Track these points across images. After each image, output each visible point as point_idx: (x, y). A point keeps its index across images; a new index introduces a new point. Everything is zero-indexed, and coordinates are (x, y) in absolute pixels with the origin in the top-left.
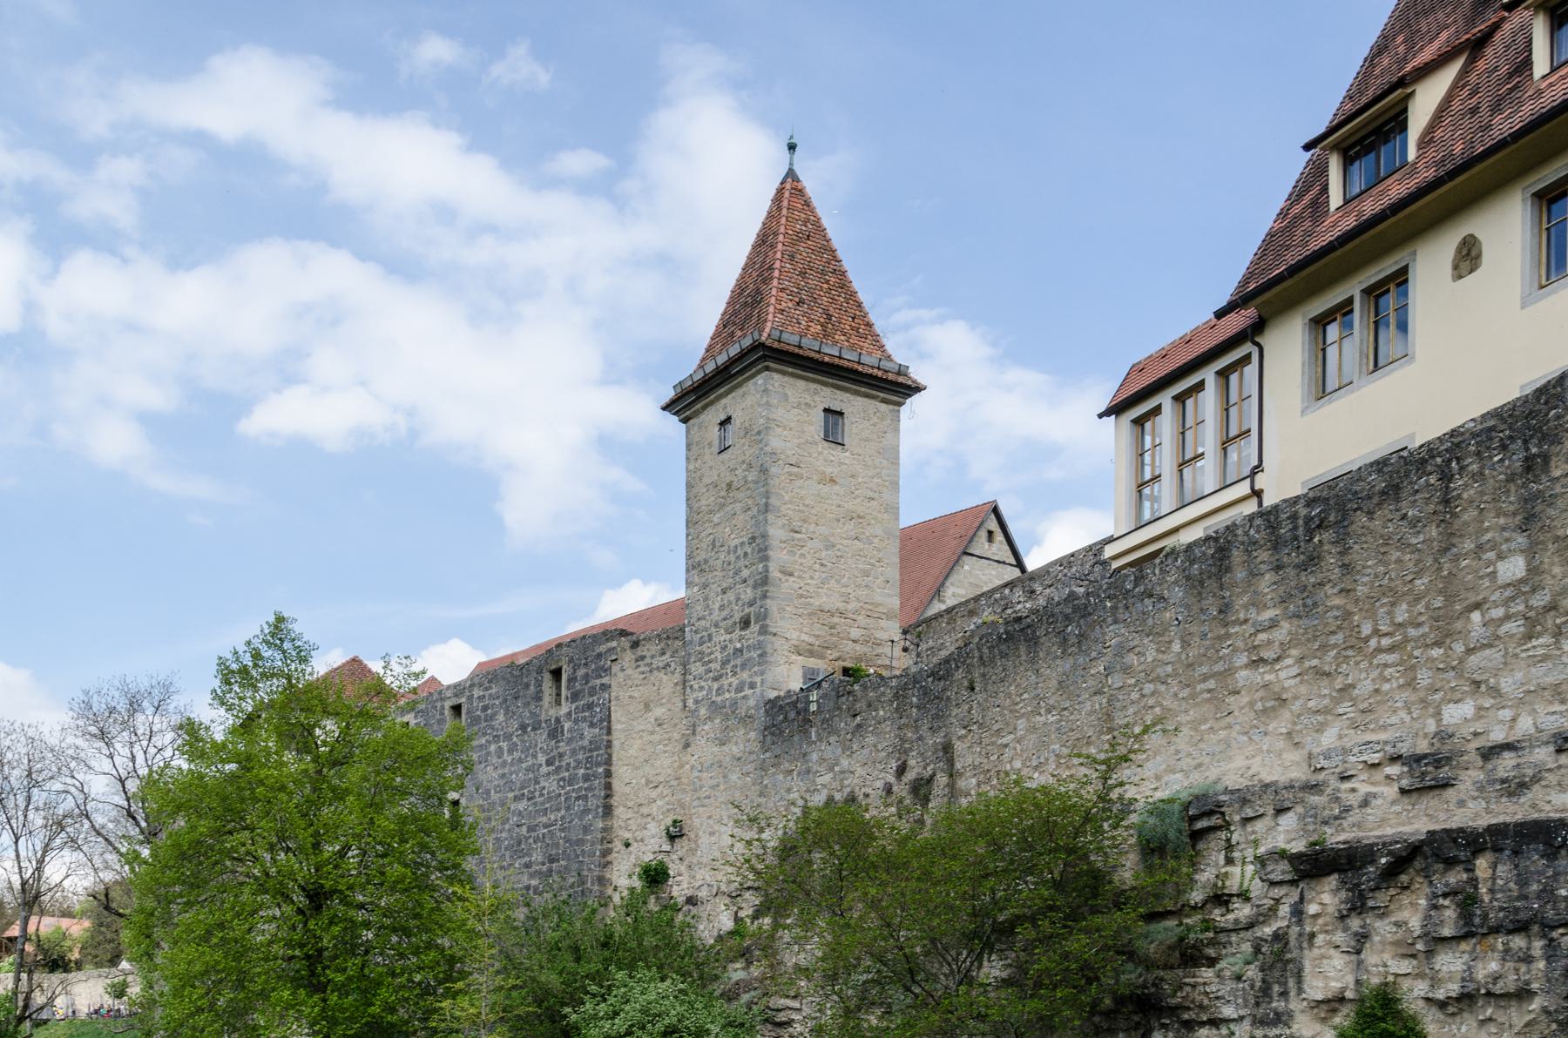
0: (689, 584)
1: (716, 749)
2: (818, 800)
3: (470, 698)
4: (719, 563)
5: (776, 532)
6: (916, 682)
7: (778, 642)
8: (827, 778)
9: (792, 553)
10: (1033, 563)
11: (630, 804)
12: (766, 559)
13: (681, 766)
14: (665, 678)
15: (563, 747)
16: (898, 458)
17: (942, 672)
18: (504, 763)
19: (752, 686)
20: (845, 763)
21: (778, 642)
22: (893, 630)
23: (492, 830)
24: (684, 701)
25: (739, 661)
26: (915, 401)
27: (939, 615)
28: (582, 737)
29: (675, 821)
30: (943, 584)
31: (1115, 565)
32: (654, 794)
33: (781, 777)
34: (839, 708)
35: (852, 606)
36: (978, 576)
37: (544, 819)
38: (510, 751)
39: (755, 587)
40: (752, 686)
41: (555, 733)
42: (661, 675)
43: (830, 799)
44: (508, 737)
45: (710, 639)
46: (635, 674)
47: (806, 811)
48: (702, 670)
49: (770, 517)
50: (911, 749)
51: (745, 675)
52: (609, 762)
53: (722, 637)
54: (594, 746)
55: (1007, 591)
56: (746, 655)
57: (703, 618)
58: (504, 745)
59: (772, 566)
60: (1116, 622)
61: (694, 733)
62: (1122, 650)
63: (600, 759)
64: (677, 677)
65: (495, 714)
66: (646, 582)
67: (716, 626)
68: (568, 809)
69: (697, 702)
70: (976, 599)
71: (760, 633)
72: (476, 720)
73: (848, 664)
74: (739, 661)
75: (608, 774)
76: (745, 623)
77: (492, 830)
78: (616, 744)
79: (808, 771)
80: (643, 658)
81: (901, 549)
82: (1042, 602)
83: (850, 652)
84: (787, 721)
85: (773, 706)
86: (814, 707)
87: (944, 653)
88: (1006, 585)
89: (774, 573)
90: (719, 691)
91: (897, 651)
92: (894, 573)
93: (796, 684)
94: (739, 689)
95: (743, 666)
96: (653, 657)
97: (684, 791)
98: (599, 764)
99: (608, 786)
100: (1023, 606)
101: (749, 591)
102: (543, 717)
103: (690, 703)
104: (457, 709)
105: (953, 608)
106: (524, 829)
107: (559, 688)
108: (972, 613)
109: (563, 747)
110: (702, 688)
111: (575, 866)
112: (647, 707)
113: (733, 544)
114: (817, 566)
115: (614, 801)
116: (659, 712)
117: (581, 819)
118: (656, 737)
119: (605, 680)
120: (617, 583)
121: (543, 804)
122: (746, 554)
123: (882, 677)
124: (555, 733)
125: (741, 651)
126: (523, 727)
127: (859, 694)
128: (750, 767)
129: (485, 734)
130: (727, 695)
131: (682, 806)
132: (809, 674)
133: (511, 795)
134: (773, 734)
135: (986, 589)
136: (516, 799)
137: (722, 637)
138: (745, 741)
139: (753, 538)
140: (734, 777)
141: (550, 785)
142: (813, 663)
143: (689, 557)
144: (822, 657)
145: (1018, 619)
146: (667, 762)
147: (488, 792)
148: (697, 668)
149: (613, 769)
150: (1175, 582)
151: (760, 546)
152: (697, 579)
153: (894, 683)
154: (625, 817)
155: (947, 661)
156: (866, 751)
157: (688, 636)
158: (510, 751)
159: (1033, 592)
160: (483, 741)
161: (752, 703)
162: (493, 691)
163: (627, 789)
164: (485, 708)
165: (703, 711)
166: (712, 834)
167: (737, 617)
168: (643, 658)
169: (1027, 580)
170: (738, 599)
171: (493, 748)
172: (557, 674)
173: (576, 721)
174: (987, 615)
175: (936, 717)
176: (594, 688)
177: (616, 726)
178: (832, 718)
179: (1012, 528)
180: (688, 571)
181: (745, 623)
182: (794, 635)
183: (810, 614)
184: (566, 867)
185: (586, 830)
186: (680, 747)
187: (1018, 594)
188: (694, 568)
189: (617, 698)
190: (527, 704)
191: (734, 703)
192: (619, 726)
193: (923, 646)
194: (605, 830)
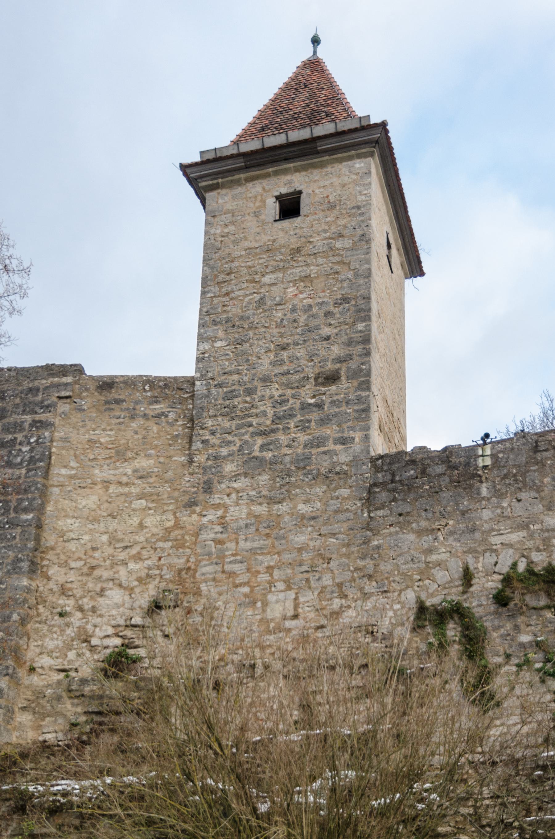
14: (155, 428)
40: (343, 441)
71: (360, 387)
79: (473, 530)
116: (142, 463)
118: (134, 490)
168: (118, 402)
181: (332, 378)
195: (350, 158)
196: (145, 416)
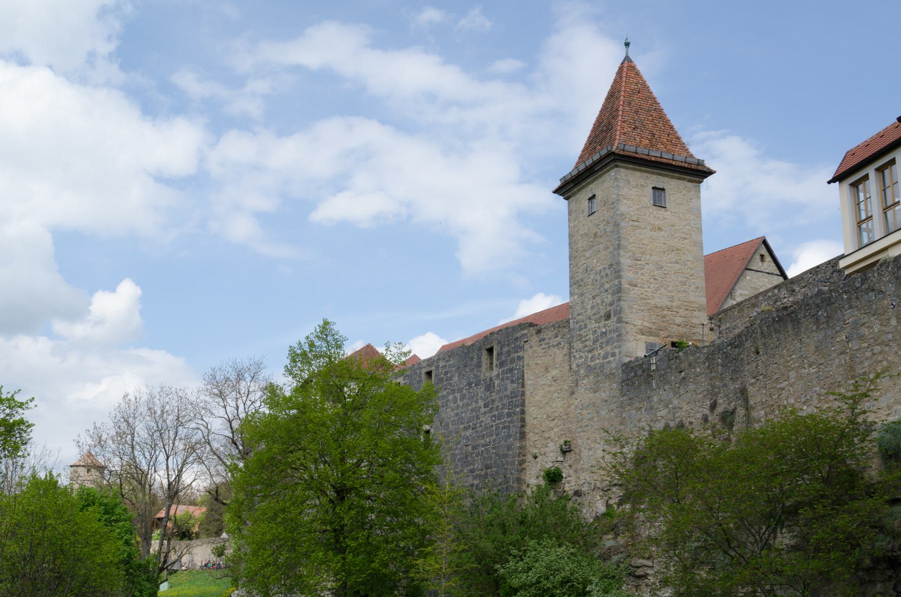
0: (572, 294)
1: (591, 395)
2: (659, 426)
3: (437, 367)
4: (590, 280)
5: (625, 261)
6: (720, 349)
7: (629, 328)
8: (664, 412)
9: (636, 273)
10: (791, 273)
11: (536, 431)
12: (620, 277)
13: (569, 406)
15: (494, 396)
16: (700, 214)
17: (737, 343)
18: (458, 407)
19: (613, 355)
20: (676, 402)
21: (629, 328)
22: (703, 318)
23: (450, 449)
24: (570, 366)
25: (604, 340)
26: (710, 179)
27: (733, 307)
28: (506, 389)
29: (566, 442)
30: (733, 289)
31: (847, 272)
32: (552, 425)
33: (634, 412)
34: (670, 368)
35: (674, 304)
36: (758, 281)
37: (483, 442)
38: (462, 399)
39: (613, 294)
40: (613, 355)
41: (489, 387)
42: (556, 350)
43: (667, 426)
44: (460, 390)
45: (586, 327)
46: (540, 350)
47: (651, 434)
48: (581, 346)
49: (622, 252)
50: (719, 393)
51: (608, 349)
52: (523, 404)
53: (593, 325)
54: (514, 394)
55: (776, 291)
56: (609, 336)
57: (581, 314)
58: (458, 395)
59: (624, 281)
60: (851, 307)
61: (577, 385)
62: (856, 325)
63: (518, 402)
64: (565, 351)
65: (453, 376)
66: (547, 294)
67: (589, 318)
68: (497, 435)
69: (578, 366)
70: (756, 297)
72: (441, 380)
73: (675, 340)
74: (604, 340)
75: (523, 412)
76: (608, 316)
77: (450, 449)
78: (527, 393)
79: (652, 408)
80: (544, 340)
81: (706, 267)
82: (800, 297)
83: (676, 333)
84: (637, 377)
85: (627, 367)
86: (653, 367)
87: (737, 331)
88: (775, 287)
89: (625, 285)
90: (593, 359)
91: (707, 330)
92: (702, 283)
93: (641, 353)
94: (605, 357)
95: (607, 343)
96: (550, 339)
97: (571, 422)
98: (517, 406)
99: (523, 420)
100: (788, 300)
101: (609, 296)
102: (482, 377)
103: (574, 366)
104: (429, 374)
105: (742, 302)
106: (470, 447)
107: (492, 359)
108: (754, 305)
109: (494, 396)
110: (581, 357)
111: (502, 471)
112: (547, 370)
113: (598, 269)
114: (652, 280)
115: (527, 429)
116: (554, 372)
117: (505, 441)
118: (553, 388)
119: (520, 354)
120: (529, 296)
121: (481, 431)
122: (607, 275)
123: (697, 347)
124: (489, 387)
125: (605, 333)
126: (469, 384)
127: (683, 358)
128: (614, 406)
129: (446, 389)
130: (597, 361)
131: (570, 432)
132: (649, 346)
133: (462, 426)
134: (627, 385)
135: (761, 290)
136: (465, 429)
137: (593, 325)
138: (610, 389)
139: (611, 265)
140: (603, 413)
141: (486, 419)
142: (651, 339)
143: (571, 278)
144: (657, 335)
145: (786, 308)
146: (560, 404)
147: (447, 425)
148: (578, 345)
149: (526, 409)
150: (889, 281)
151: (616, 270)
152: (576, 291)
153: (705, 350)
154: (533, 439)
155: (739, 336)
156: (688, 395)
157: (571, 325)
158: (462, 399)
159: (793, 291)
160: (445, 393)
161: (613, 365)
162: (451, 362)
163: (535, 422)
164: (446, 373)
165: (582, 372)
166: (590, 449)
167: (602, 313)
169: (788, 284)
170: (603, 302)
171: (451, 397)
172: (490, 351)
173: (502, 380)
174: (764, 307)
175: (735, 371)
176: (513, 359)
177: (528, 382)
178: (665, 374)
179: (777, 254)
180: (571, 286)
181: (608, 316)
182: (639, 323)
183: (648, 310)
184: (496, 472)
185: (509, 448)
186: (567, 394)
187: (784, 292)
188: (575, 284)
189: (528, 365)
190: (472, 370)
191: (602, 366)
192: (529, 382)
193: (723, 327)
194: (521, 448)
195: (608, 171)
196: (553, 346)
